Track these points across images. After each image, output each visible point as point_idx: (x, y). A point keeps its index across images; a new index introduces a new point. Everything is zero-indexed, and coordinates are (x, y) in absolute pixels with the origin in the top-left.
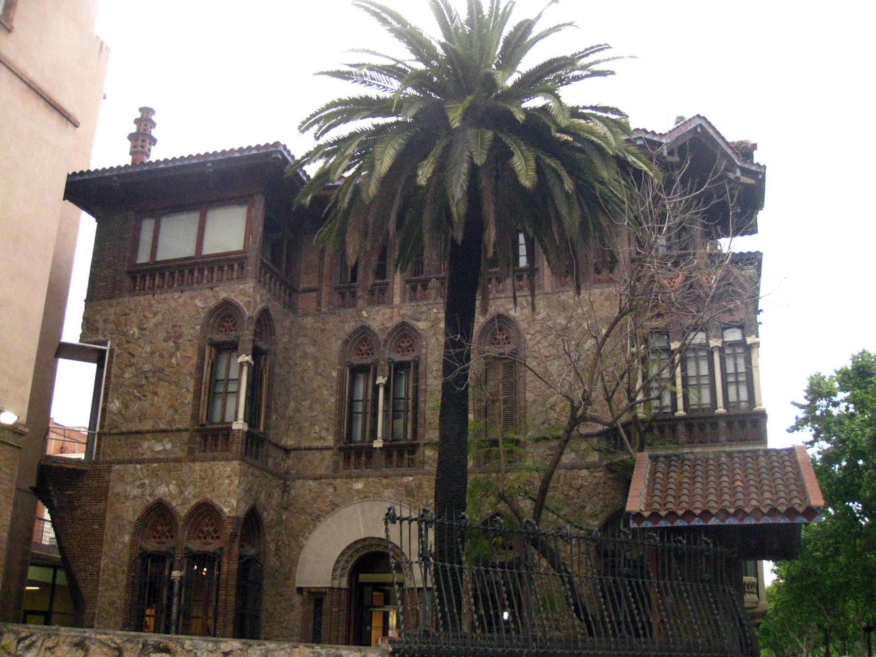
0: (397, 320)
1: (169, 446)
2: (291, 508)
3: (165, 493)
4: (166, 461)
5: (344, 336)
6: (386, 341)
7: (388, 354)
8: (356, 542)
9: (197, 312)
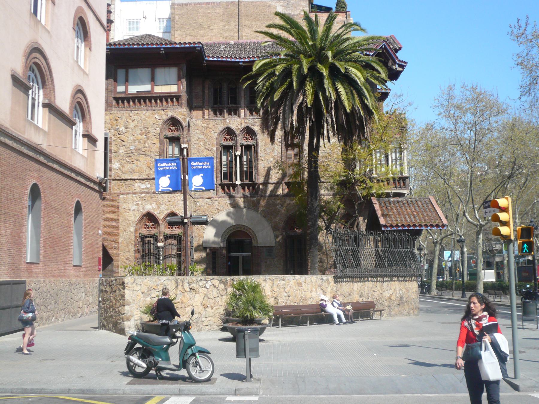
0: (244, 125)
1: (149, 186)
3: (150, 208)
4: (149, 193)
5: (219, 131)
7: (241, 140)
9: (157, 122)
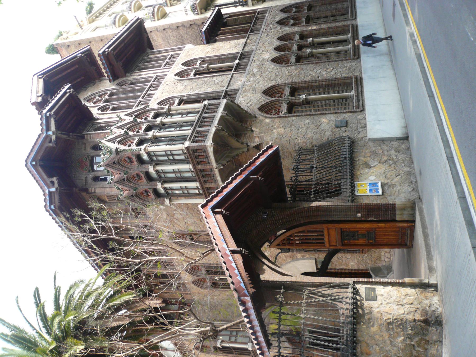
6: (197, 276)
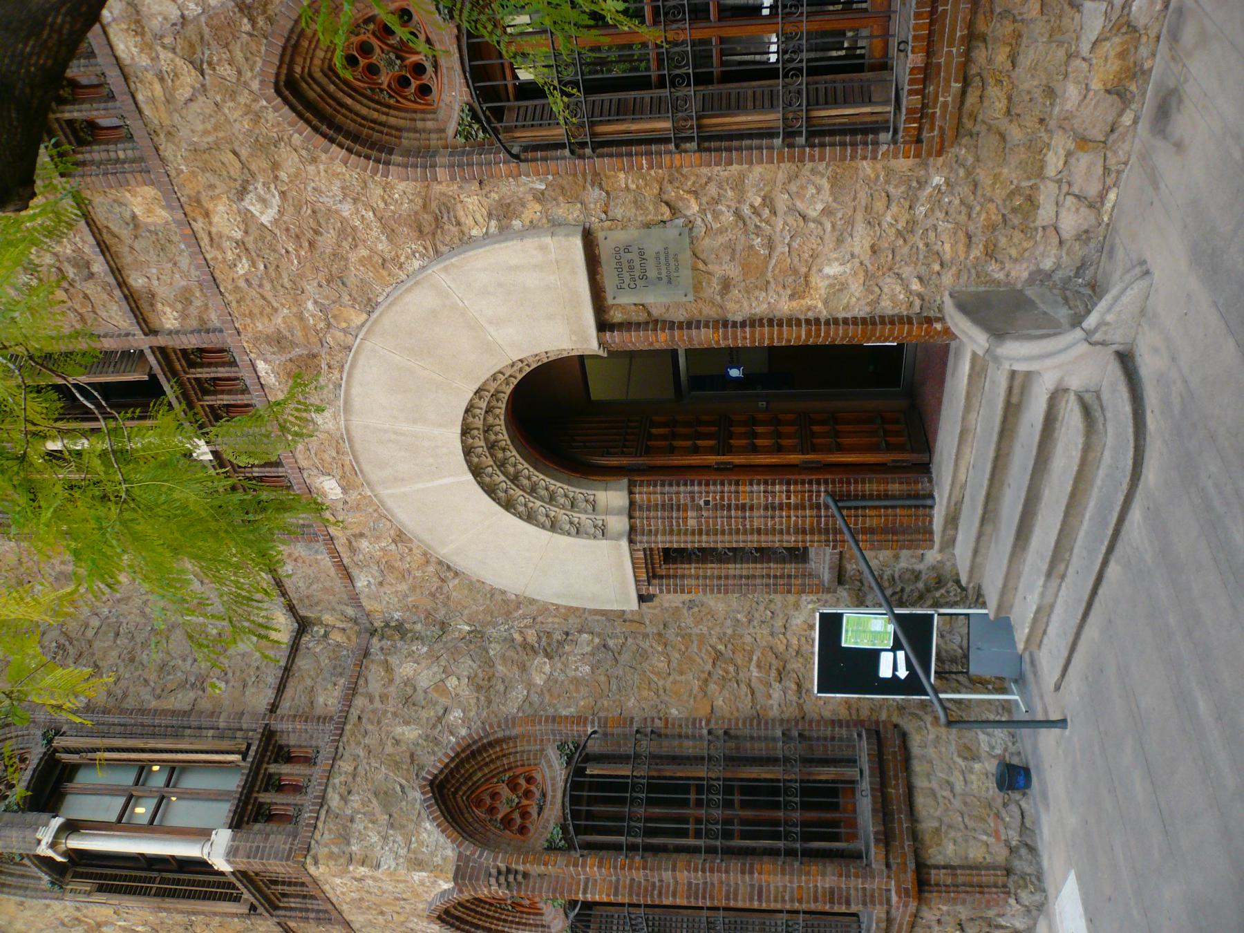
2: (441, 614)
8: (490, 491)
